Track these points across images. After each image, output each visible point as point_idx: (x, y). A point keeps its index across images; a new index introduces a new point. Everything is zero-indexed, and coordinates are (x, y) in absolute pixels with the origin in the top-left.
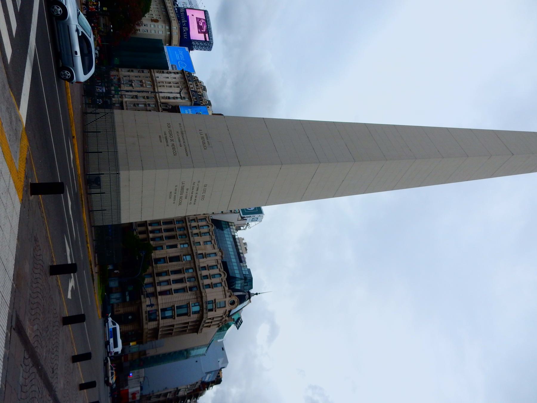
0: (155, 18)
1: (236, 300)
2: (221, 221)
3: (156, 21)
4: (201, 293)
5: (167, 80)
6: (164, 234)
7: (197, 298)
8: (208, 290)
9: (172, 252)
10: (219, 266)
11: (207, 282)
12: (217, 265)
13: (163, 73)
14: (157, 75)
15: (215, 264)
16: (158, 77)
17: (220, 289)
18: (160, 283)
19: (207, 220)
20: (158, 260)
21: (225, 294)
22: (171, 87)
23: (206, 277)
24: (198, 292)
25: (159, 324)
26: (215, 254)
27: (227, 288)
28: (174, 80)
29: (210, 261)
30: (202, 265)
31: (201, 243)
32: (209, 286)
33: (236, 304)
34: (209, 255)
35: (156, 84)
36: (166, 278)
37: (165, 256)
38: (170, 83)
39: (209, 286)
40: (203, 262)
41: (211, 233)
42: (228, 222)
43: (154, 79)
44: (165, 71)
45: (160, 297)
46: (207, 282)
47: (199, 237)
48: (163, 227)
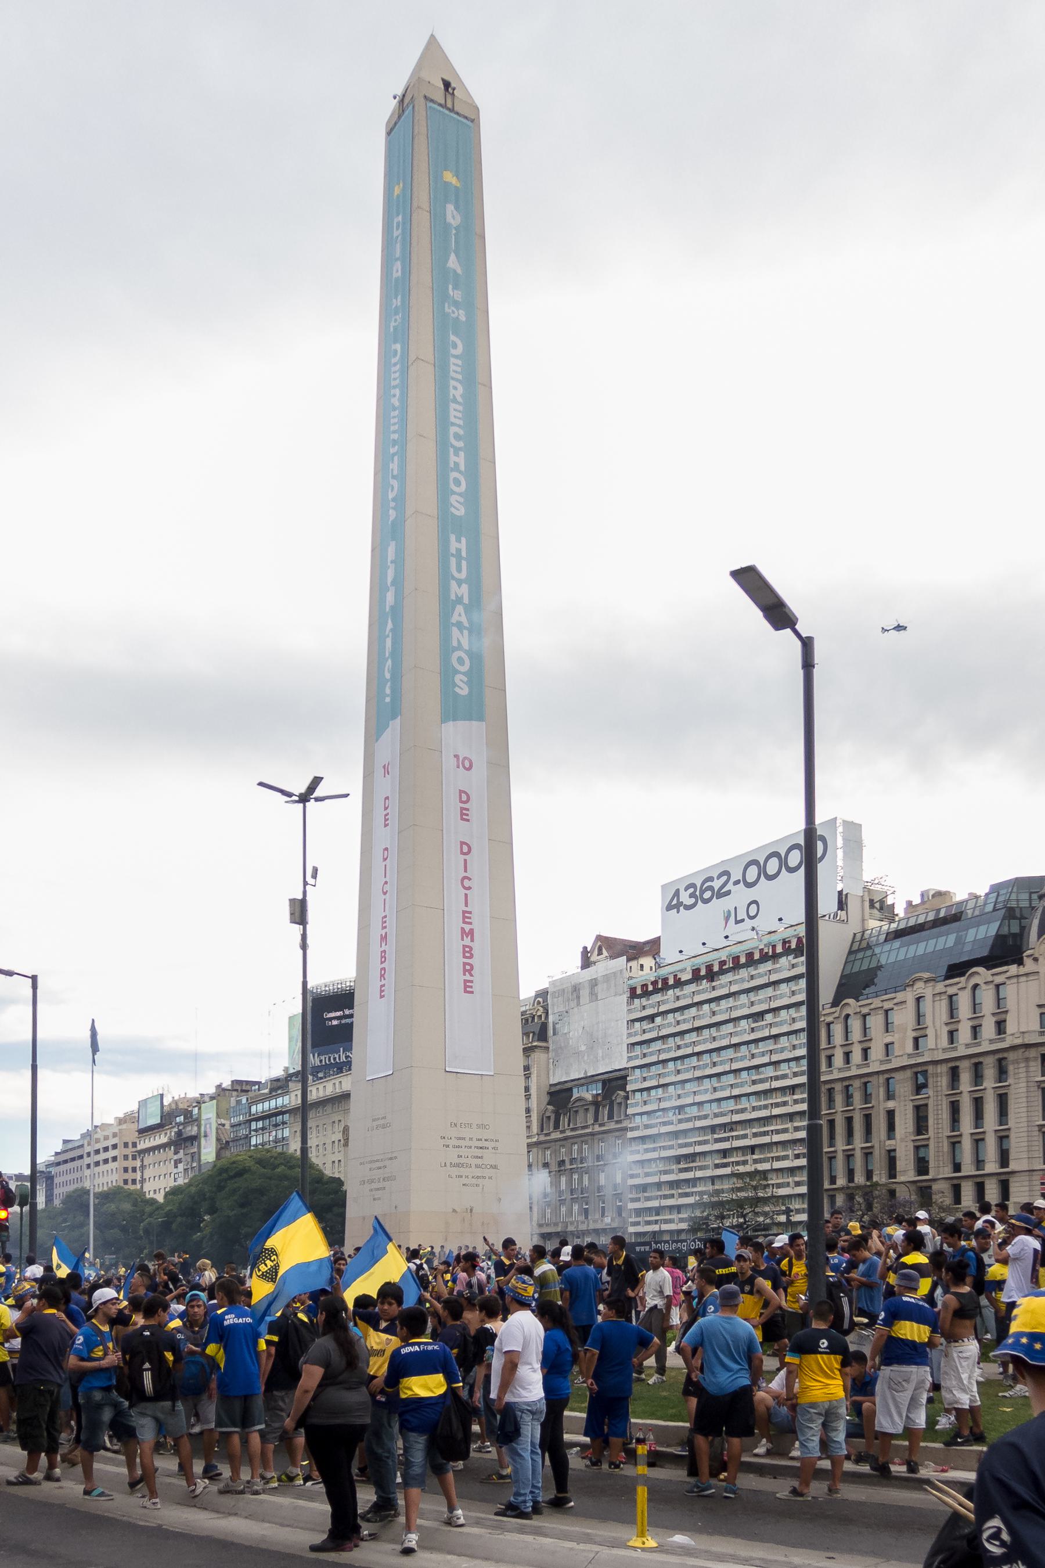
2: (842, 977)
4: (1013, 1048)
6: (859, 1143)
7: (1027, 1060)
9: (905, 1123)
15: (944, 1004)
21: (1027, 975)
26: (918, 999)
27: (1013, 969)
30: (944, 1042)
31: (888, 1040)
34: (919, 1016)
37: (911, 1145)
42: (850, 952)
45: (1013, 1166)
47: (872, 1044)
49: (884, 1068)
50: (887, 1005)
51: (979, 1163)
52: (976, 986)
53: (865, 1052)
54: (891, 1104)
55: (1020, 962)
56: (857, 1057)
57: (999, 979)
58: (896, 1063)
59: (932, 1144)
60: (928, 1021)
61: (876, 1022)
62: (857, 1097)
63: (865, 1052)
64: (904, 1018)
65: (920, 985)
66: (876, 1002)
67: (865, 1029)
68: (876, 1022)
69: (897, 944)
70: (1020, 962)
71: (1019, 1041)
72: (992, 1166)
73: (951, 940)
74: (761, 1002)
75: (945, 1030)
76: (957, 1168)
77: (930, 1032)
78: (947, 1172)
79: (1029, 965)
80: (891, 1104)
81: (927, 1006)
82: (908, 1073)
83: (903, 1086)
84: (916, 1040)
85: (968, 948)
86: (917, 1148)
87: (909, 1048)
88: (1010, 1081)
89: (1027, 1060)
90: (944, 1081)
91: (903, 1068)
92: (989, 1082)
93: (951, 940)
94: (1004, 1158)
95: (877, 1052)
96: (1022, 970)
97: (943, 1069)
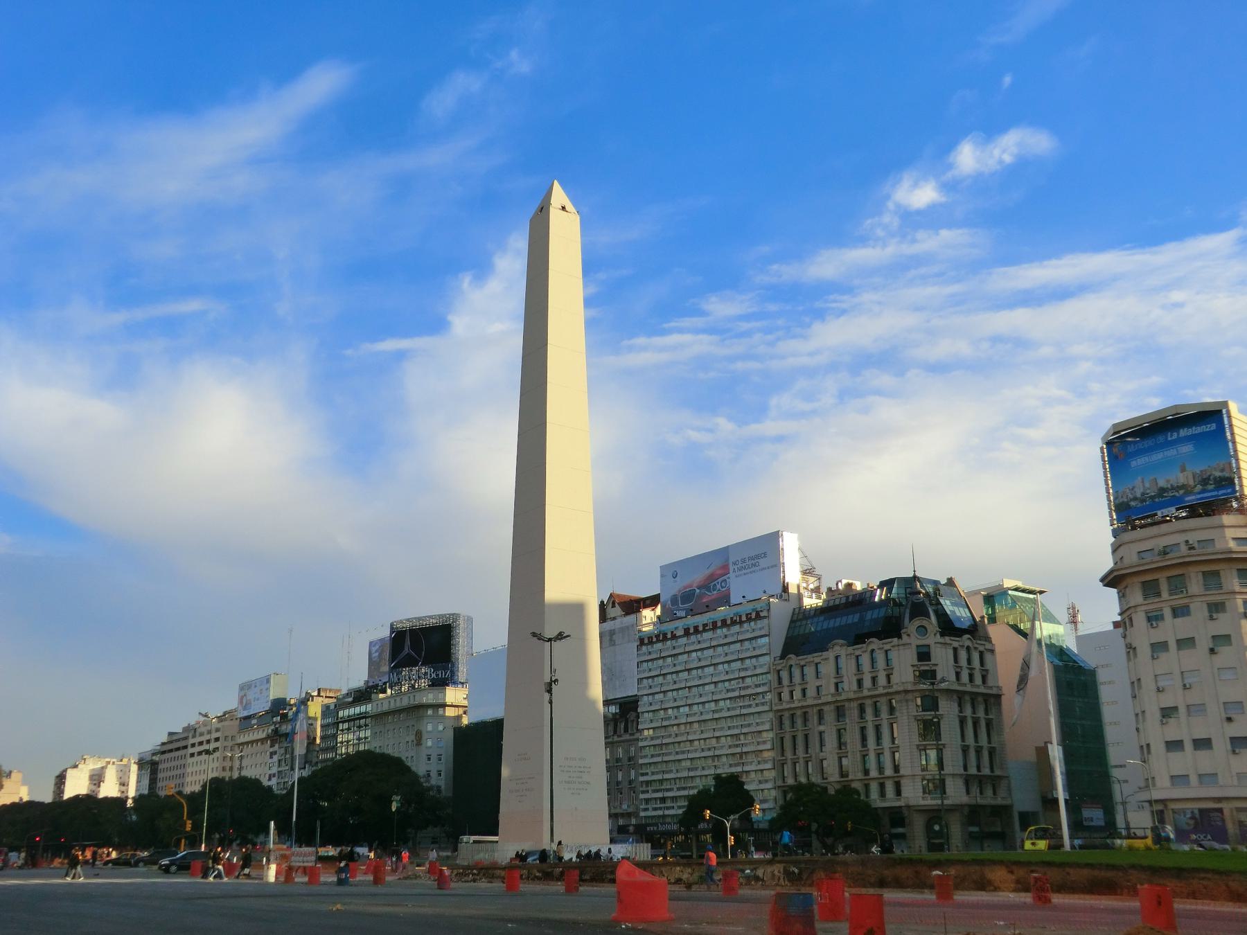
0: (413, 737)
1: (917, 622)
2: (787, 638)
3: (419, 735)
4: (897, 693)
7: (907, 701)
8: (894, 679)
10: (857, 653)
11: (882, 680)
12: (857, 657)
15: (854, 661)
18: (881, 769)
20: (843, 774)
23: (874, 679)
24: (898, 697)
25: (953, 775)
26: (837, 658)
27: (895, 640)
29: (848, 667)
30: (855, 687)
32: (888, 677)
33: (925, 623)
34: (838, 669)
36: (872, 758)
40: (849, 685)
41: (802, 663)
45: (902, 772)
46: (882, 680)
47: (808, 686)
48: (789, 755)
49: (816, 702)
50: (817, 660)
51: (881, 769)
52: (873, 651)
53: (804, 691)
54: (822, 728)
55: (900, 637)
56: (797, 694)
57: (887, 647)
58: (823, 700)
60: (843, 672)
61: (809, 671)
62: (799, 721)
63: (804, 691)
64: (828, 669)
65: (837, 648)
66: (810, 658)
67: (803, 675)
68: (809, 671)
69: (822, 618)
70: (900, 637)
71: (901, 689)
72: (889, 772)
73: (856, 618)
74: (732, 653)
75: (854, 679)
76: (866, 772)
77: (845, 679)
78: (860, 775)
79: (905, 639)
80: (822, 728)
81: (842, 662)
82: (832, 707)
83: (830, 716)
84: (837, 684)
85: (867, 624)
86: (840, 759)
87: (832, 690)
88: (897, 714)
89: (907, 701)
90: (856, 712)
92: (884, 715)
93: (856, 618)
94: (896, 768)
95: (811, 692)
96: (901, 642)
97: (855, 705)
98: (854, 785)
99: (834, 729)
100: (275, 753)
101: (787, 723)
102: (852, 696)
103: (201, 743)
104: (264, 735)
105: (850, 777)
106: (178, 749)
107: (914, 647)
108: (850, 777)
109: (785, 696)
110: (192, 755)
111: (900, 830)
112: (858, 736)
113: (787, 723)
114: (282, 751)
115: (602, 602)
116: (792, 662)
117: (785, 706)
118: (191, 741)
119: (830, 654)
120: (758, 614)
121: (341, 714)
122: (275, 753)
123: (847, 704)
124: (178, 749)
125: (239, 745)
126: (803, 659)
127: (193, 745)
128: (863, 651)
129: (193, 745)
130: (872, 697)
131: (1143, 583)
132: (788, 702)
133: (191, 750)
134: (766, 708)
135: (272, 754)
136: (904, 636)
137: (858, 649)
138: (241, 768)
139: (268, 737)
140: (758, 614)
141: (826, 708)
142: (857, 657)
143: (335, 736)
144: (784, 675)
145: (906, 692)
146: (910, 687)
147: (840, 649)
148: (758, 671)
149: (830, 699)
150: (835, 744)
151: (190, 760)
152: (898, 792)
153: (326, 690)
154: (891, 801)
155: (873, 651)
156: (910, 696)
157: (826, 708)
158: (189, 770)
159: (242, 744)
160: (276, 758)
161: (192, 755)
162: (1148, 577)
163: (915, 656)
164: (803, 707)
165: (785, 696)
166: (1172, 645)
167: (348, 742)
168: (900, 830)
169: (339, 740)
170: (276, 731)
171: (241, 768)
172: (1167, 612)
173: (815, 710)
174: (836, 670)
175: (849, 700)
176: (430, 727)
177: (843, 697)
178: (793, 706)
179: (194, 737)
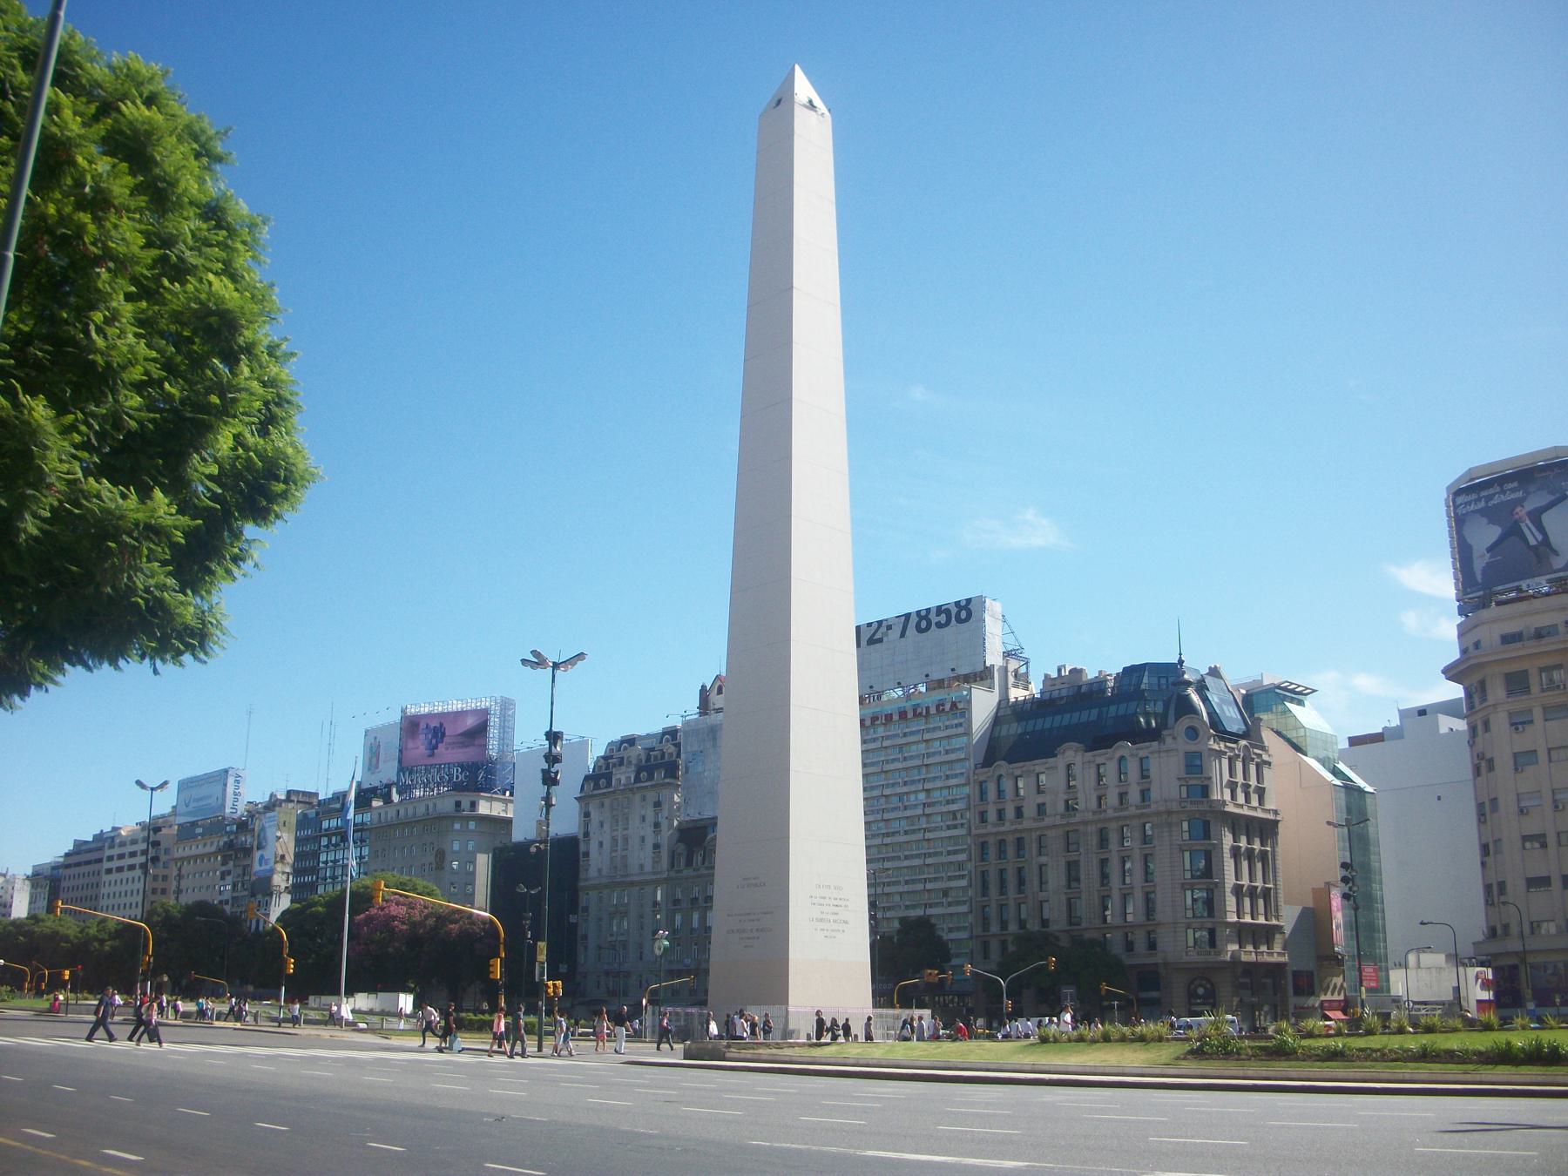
0: (432, 859)
3: (441, 857)
4: (1158, 813)
5: (607, 845)
7: (1170, 825)
8: (1154, 795)
10: (1099, 760)
12: (1098, 766)
13: (587, 854)
14: (593, 872)
15: (1093, 771)
16: (600, 870)
17: (1154, 766)
19: (982, 778)
20: (1072, 918)
22: (626, 839)
23: (1122, 796)
26: (1069, 766)
27: (1155, 744)
28: (607, 827)
29: (1085, 781)
32: (1144, 794)
33: (1196, 724)
35: (618, 879)
38: (615, 840)
39: (1144, 794)
41: (1018, 772)
43: (604, 881)
44: (582, 848)
49: (1035, 825)
54: (1043, 859)
58: (1048, 821)
59: (1084, 896)
71: (1162, 808)
80: (1043, 859)
81: (1077, 770)
88: (1155, 842)
89: (1170, 825)
90: (1094, 841)
91: (1055, 826)
96: (1164, 747)
98: (1087, 936)
99: (1062, 863)
100: (229, 873)
101: (992, 852)
102: (1090, 816)
103: (121, 856)
104: (213, 849)
105: (1084, 925)
106: (88, 863)
107: (1181, 754)
108: (1084, 925)
109: (992, 816)
110: (109, 871)
111: (1154, 994)
112: (1096, 872)
113: (992, 852)
114: (240, 870)
115: (703, 687)
116: (1002, 771)
117: (990, 829)
118: (108, 853)
119: (1060, 762)
120: (954, 705)
121: (325, 824)
122: (229, 873)
123: (1081, 828)
124: (88, 863)
125: (176, 860)
126: (1017, 769)
127: (110, 858)
128: (1108, 760)
129: (110, 858)
130: (1118, 818)
131: (1507, 675)
132: (995, 825)
133: (107, 865)
134: (962, 832)
135: (223, 876)
136: (1169, 740)
137: (1100, 756)
138: (179, 891)
139: (219, 850)
140: (954, 705)
141: (1050, 833)
142: (1098, 766)
143: (316, 855)
144: (991, 788)
145: (1170, 813)
146: (1175, 807)
147: (1071, 754)
148: (953, 782)
149: (1058, 821)
150: (1063, 882)
151: (106, 878)
152: (1152, 946)
153: (297, 792)
154: (1141, 956)
155: (1122, 758)
156: (1174, 818)
157: (1050, 833)
158: (104, 891)
159: (182, 859)
160: (229, 879)
161: (109, 871)
162: (1515, 667)
163: (1183, 767)
164: (1016, 831)
165: (992, 816)
166: (1542, 756)
167: (335, 861)
168: (1154, 994)
169: (323, 857)
170: (230, 845)
171: (179, 891)
172: (1537, 714)
173: (1034, 835)
174: (1067, 779)
175: (1086, 823)
176: (456, 847)
177: (1078, 818)
178: (1002, 829)
179: (112, 847)
